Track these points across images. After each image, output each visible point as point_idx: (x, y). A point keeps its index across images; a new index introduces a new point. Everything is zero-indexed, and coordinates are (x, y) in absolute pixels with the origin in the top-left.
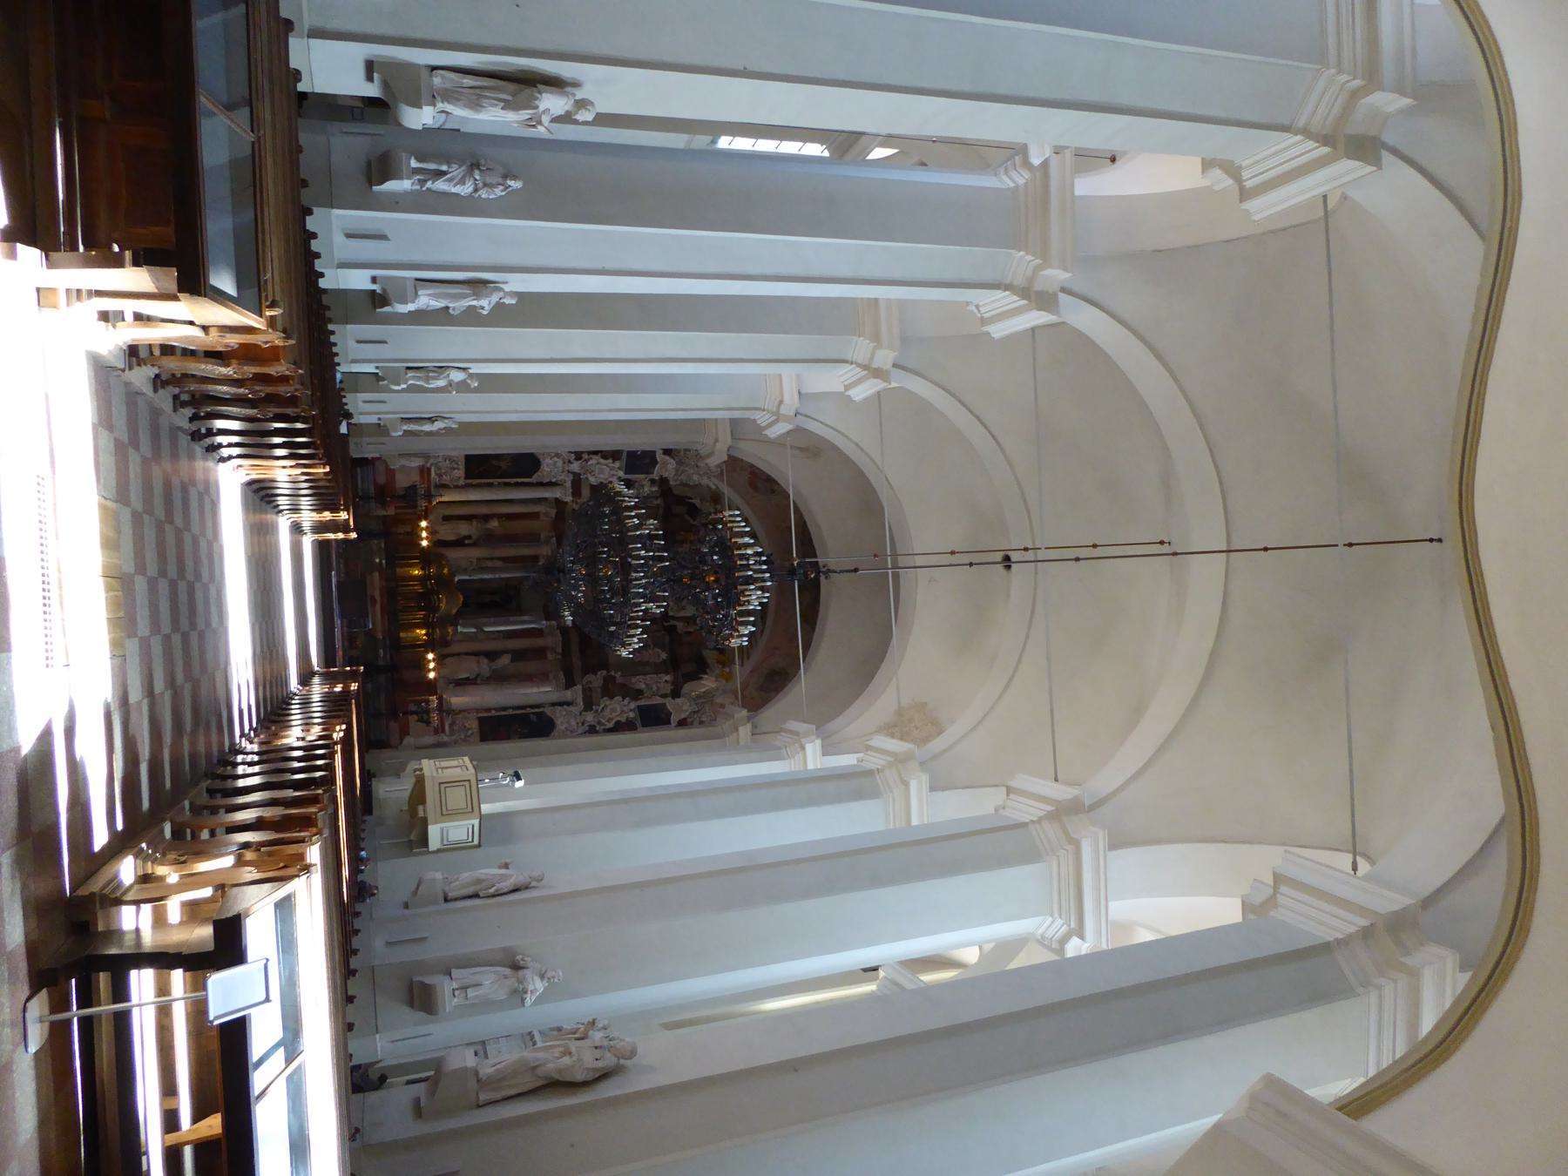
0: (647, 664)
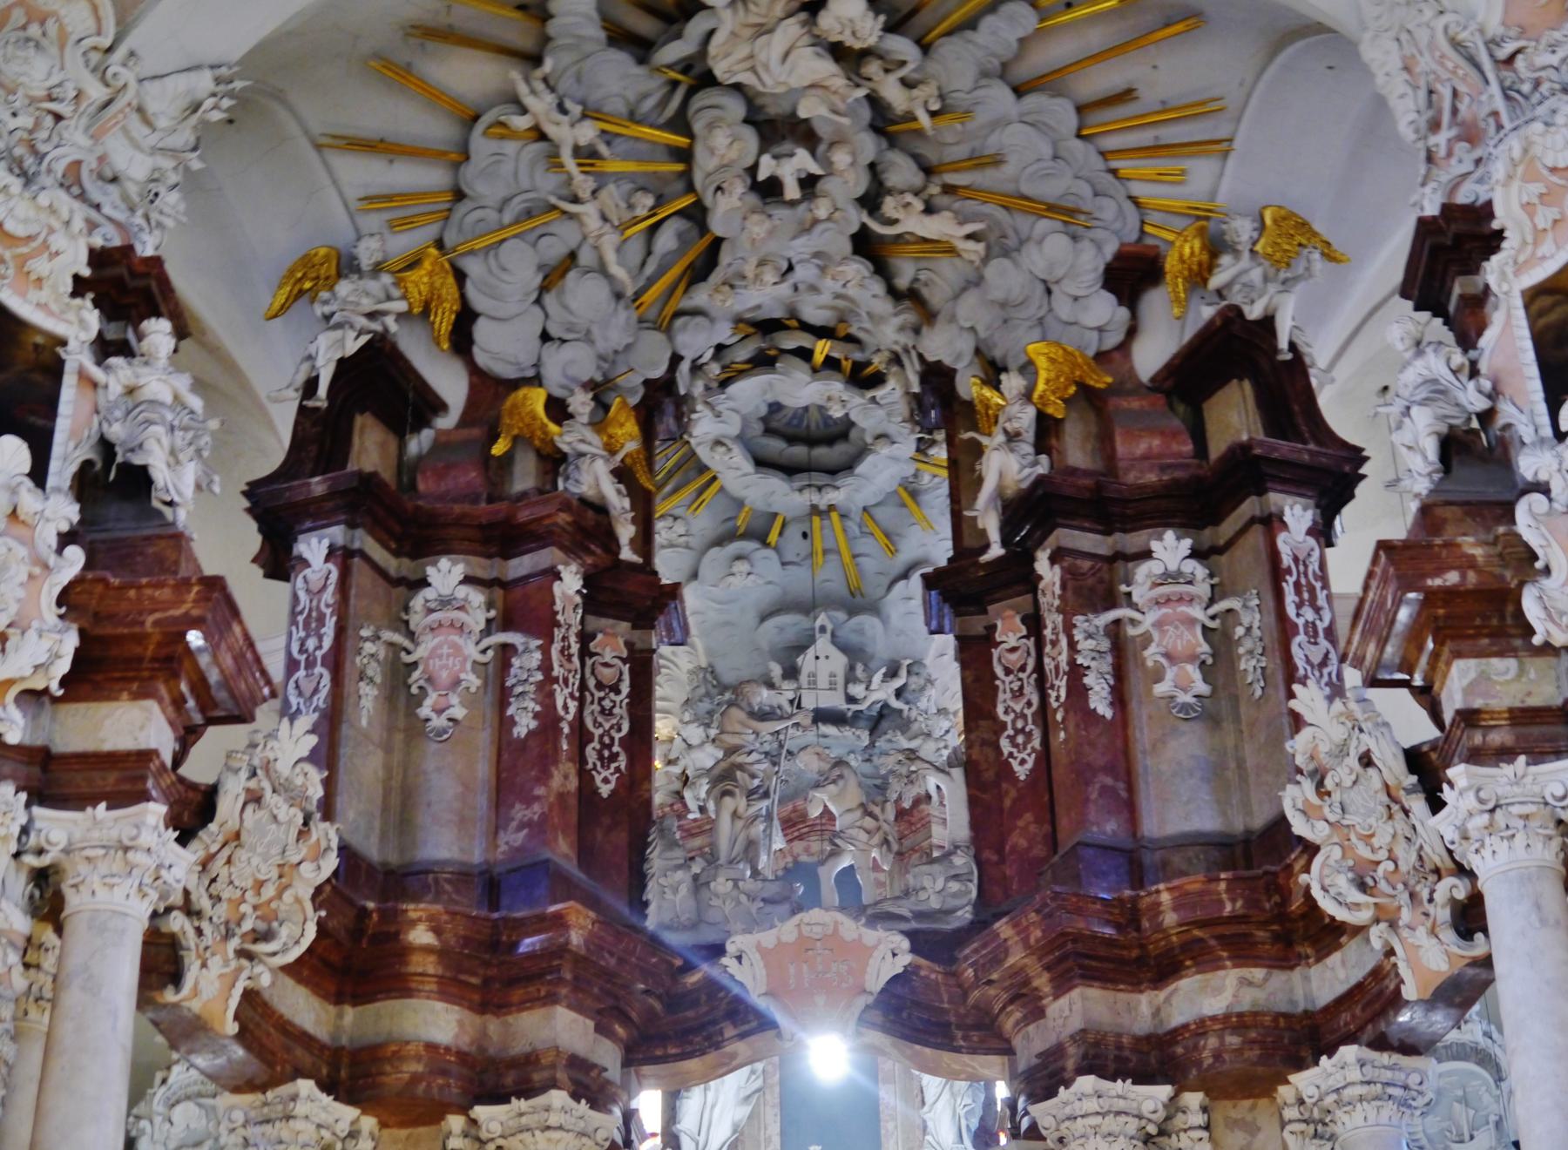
0: (1220, 638)
